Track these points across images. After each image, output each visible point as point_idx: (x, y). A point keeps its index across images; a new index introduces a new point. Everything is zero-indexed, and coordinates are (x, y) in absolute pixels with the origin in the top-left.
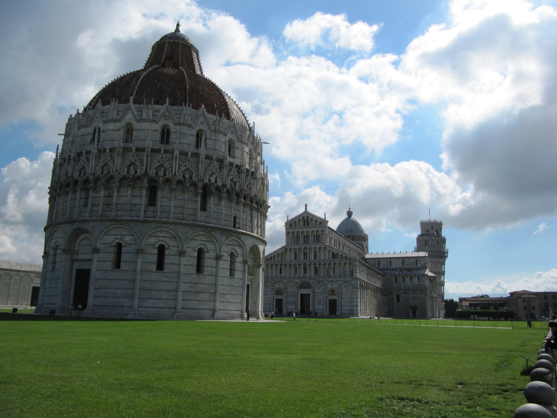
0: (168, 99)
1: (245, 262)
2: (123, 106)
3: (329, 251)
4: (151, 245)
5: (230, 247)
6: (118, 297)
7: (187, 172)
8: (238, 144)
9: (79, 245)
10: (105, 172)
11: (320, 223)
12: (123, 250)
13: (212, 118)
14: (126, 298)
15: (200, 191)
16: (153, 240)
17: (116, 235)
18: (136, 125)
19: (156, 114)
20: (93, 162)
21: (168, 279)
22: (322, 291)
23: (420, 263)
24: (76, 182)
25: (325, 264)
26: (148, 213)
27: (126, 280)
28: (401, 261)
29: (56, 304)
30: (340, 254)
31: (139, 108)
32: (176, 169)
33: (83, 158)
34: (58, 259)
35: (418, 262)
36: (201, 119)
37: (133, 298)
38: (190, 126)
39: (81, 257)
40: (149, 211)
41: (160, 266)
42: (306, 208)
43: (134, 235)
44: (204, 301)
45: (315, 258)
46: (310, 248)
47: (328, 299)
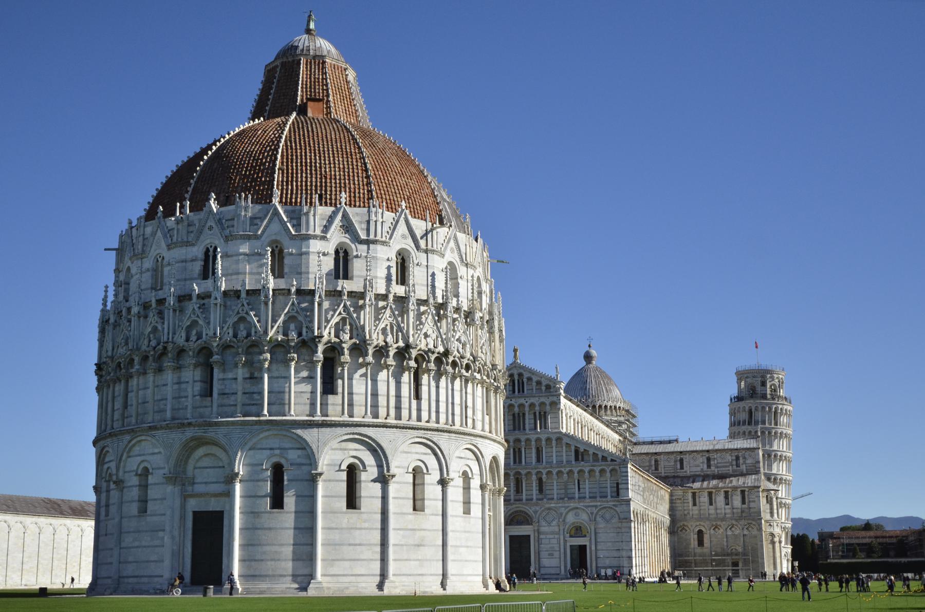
1: (483, 487)
5: (464, 462)
8: (462, 271)
9: (195, 468)
10: (242, 333)
11: (548, 387)
13: (419, 226)
15: (412, 364)
17: (271, 449)
20: (215, 315)
22: (556, 529)
23: (744, 463)
24: (181, 352)
25: (560, 473)
28: (702, 460)
29: (162, 576)
31: (293, 211)
33: (193, 305)
34: (152, 493)
35: (741, 461)
39: (199, 488)
42: (515, 356)
43: (304, 449)
44: (427, 560)
45: (539, 459)
46: (528, 440)
47: (568, 544)
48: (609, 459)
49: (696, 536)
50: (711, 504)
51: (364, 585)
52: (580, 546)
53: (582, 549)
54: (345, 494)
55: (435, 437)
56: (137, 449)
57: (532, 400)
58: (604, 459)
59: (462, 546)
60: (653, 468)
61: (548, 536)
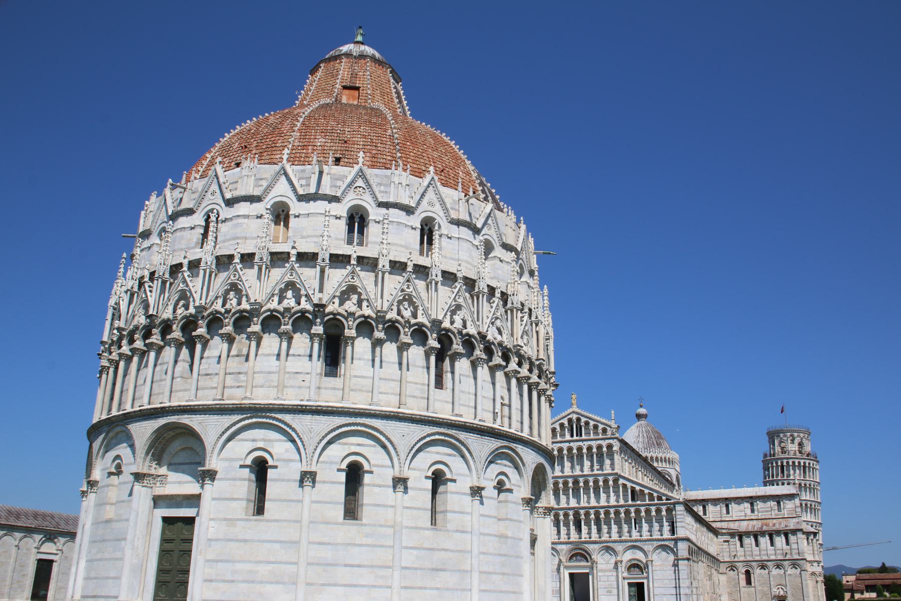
2: (269, 171)
3: (624, 486)
4: (332, 463)
6: (261, 582)
7: (406, 303)
11: (604, 431)
12: (271, 473)
13: (451, 195)
14: (277, 583)
16: (337, 451)
17: (254, 440)
18: (296, 208)
19: (339, 183)
21: (370, 541)
24: (166, 328)
26: (323, 391)
27: (276, 542)
28: (747, 505)
30: (646, 491)
31: (303, 171)
32: (382, 294)
36: (431, 195)
37: (295, 583)
38: (409, 210)
39: (171, 489)
40: (326, 388)
41: (351, 511)
44: (448, 589)
50: (757, 545)
52: (638, 583)
53: (640, 587)
54: (343, 500)
55: (462, 435)
57: (590, 443)
58: (660, 498)
59: (495, 573)
61: (606, 574)
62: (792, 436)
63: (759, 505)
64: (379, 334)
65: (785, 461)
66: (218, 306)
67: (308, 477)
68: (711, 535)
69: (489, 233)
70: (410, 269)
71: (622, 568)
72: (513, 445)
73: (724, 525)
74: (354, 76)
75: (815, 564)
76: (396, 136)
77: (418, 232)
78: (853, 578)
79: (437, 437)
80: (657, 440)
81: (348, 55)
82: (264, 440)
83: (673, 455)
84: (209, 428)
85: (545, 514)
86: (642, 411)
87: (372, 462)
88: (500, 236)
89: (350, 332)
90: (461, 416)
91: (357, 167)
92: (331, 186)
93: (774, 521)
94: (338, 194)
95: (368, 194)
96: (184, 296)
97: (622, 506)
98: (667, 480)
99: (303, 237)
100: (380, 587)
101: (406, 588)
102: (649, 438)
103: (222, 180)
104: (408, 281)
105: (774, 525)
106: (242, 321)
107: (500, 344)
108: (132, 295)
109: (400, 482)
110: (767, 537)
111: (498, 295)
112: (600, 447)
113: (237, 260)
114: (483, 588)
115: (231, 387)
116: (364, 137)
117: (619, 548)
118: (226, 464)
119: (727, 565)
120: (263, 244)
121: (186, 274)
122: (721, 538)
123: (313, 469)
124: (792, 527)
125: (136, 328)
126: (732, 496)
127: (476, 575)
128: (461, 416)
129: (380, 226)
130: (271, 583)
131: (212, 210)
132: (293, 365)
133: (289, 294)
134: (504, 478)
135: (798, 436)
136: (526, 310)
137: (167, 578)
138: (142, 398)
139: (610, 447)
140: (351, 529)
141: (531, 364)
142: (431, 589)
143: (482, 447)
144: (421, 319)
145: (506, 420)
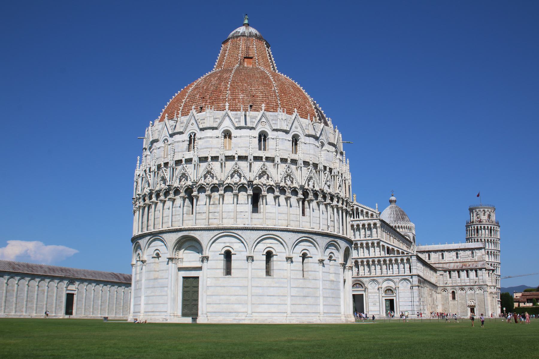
0: (263, 105)
3: (383, 246)
4: (260, 252)
11: (372, 215)
12: (233, 257)
13: (305, 122)
14: (239, 304)
18: (234, 133)
19: (254, 120)
21: (277, 285)
24: (177, 192)
28: (454, 253)
30: (396, 249)
31: (236, 114)
32: (276, 174)
36: (296, 123)
38: (287, 132)
44: (310, 305)
48: (405, 253)
49: (451, 295)
50: (459, 277)
51: (275, 318)
52: (390, 300)
53: (392, 301)
55: (315, 237)
56: (153, 244)
58: (403, 253)
60: (427, 259)
62: (484, 211)
63: (461, 253)
64: (277, 193)
65: (479, 226)
66: (202, 182)
67: (250, 258)
68: (432, 272)
69: (323, 138)
70: (289, 162)
71: (382, 291)
72: (336, 240)
73: (441, 265)
74: (248, 48)
75: (493, 288)
76: (277, 91)
77: (291, 142)
78: (520, 294)
79: (304, 238)
80: (401, 215)
81: (243, 35)
82: (229, 243)
83: (412, 225)
84: (204, 238)
85: (349, 269)
86: (393, 198)
87: (277, 251)
88: (327, 139)
89: (264, 193)
90: (314, 228)
91: (262, 112)
92: (251, 122)
93: (470, 263)
94: (254, 126)
95: (267, 125)
96: (184, 176)
97: (381, 257)
98: (407, 240)
99: (239, 147)
100: (282, 304)
101: (293, 304)
102: (397, 215)
103: (196, 118)
104: (289, 167)
105: (469, 265)
106: (215, 188)
107: (329, 194)
108: (155, 173)
109: (289, 259)
110: (465, 272)
111: (328, 170)
112: (369, 225)
113: (210, 160)
114: (325, 304)
115: (212, 219)
116: (262, 92)
117: (380, 280)
118: (213, 253)
119: (442, 288)
120: (222, 152)
121: (185, 166)
122: (439, 273)
123: (252, 255)
124: (480, 267)
125: (160, 190)
126: (445, 249)
127: (321, 299)
128: (314, 228)
129: (275, 140)
130: (237, 304)
131: (192, 133)
132: (240, 208)
133: (236, 176)
134: (332, 254)
135: (488, 211)
136: (340, 175)
137: (188, 303)
138: (167, 222)
139: (375, 224)
140: (268, 281)
141: (343, 201)
142: (304, 305)
143: (323, 241)
144: (295, 185)
145: (332, 228)
